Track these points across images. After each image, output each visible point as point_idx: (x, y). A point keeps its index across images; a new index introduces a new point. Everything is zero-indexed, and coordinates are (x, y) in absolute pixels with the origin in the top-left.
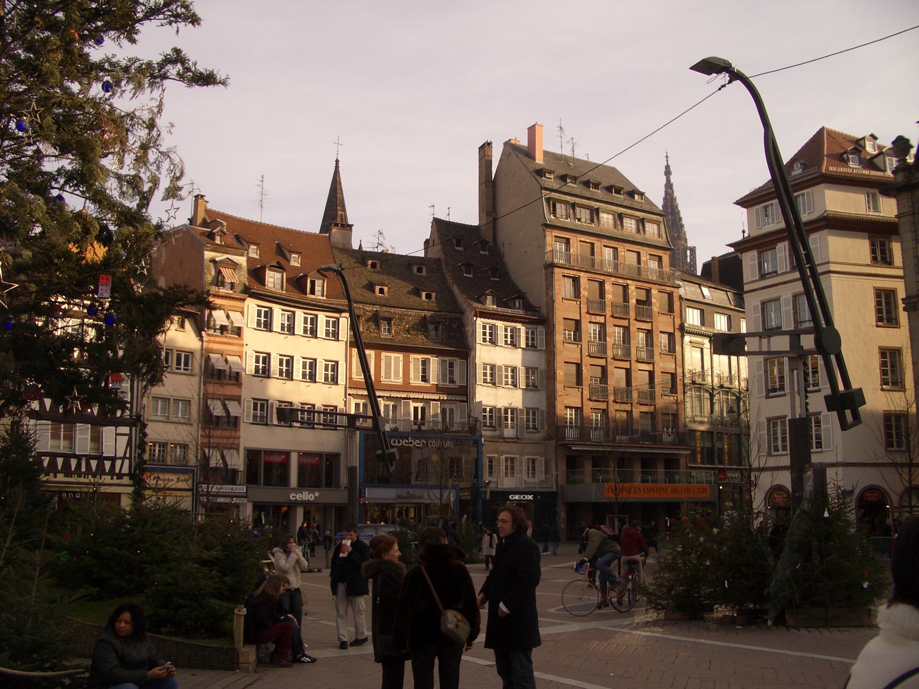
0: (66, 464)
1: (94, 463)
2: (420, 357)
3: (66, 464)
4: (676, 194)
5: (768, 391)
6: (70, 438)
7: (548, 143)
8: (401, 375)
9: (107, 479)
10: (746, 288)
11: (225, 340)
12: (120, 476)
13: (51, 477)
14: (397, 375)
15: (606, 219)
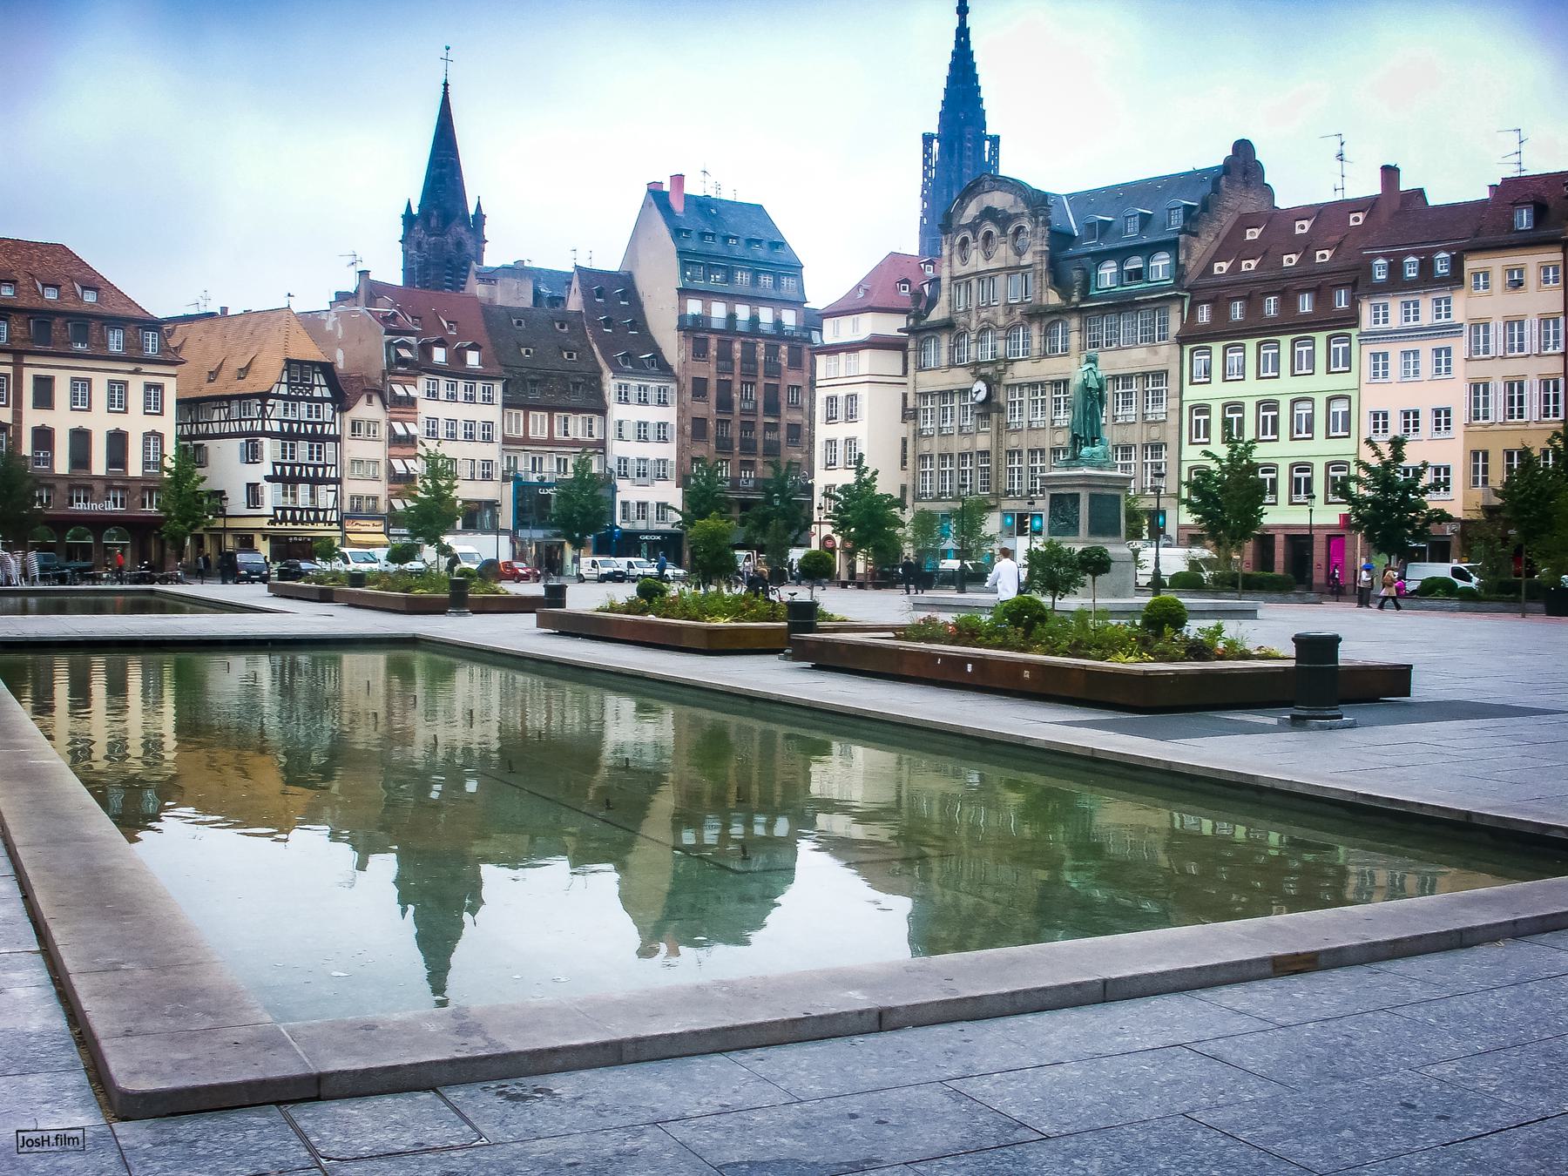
0: (293, 515)
1: (312, 514)
2: (562, 414)
3: (293, 515)
4: (974, 46)
5: (827, 465)
6: (294, 495)
7: (693, 188)
8: (546, 431)
9: (321, 526)
10: (818, 384)
11: (403, 410)
12: (331, 523)
13: (283, 526)
14: (542, 432)
15: (742, 278)
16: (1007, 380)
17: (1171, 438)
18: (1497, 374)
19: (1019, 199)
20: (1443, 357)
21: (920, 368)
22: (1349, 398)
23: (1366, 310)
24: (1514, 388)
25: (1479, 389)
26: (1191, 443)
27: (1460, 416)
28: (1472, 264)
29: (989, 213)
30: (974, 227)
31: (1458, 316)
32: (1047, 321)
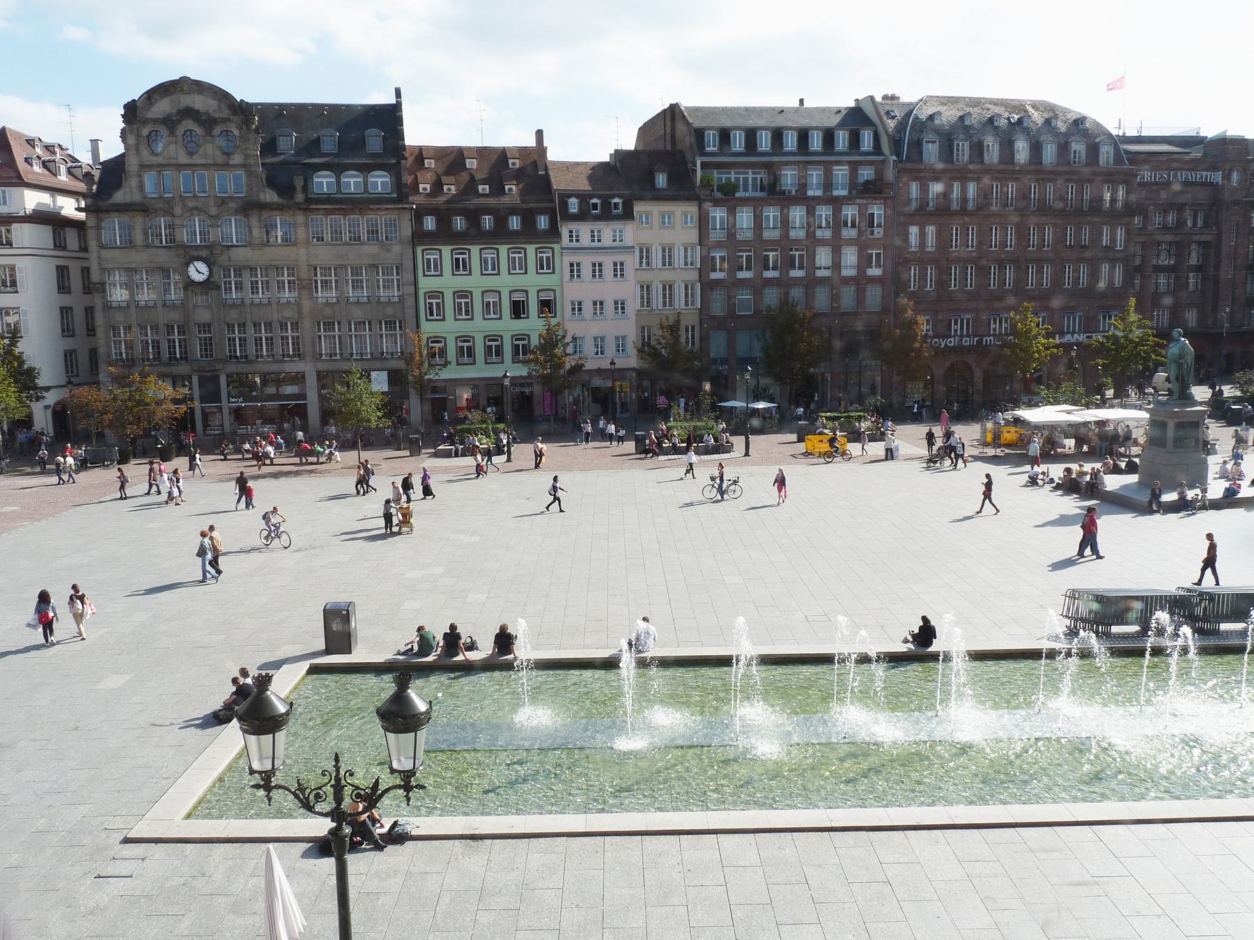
16: (223, 259)
17: (410, 313)
18: (656, 278)
19: (223, 106)
20: (619, 270)
21: (102, 247)
22: (554, 291)
23: (565, 232)
24: (668, 288)
25: (646, 288)
26: (427, 320)
27: (633, 305)
28: (639, 208)
29: (189, 113)
30: (170, 123)
31: (629, 239)
32: (265, 214)
